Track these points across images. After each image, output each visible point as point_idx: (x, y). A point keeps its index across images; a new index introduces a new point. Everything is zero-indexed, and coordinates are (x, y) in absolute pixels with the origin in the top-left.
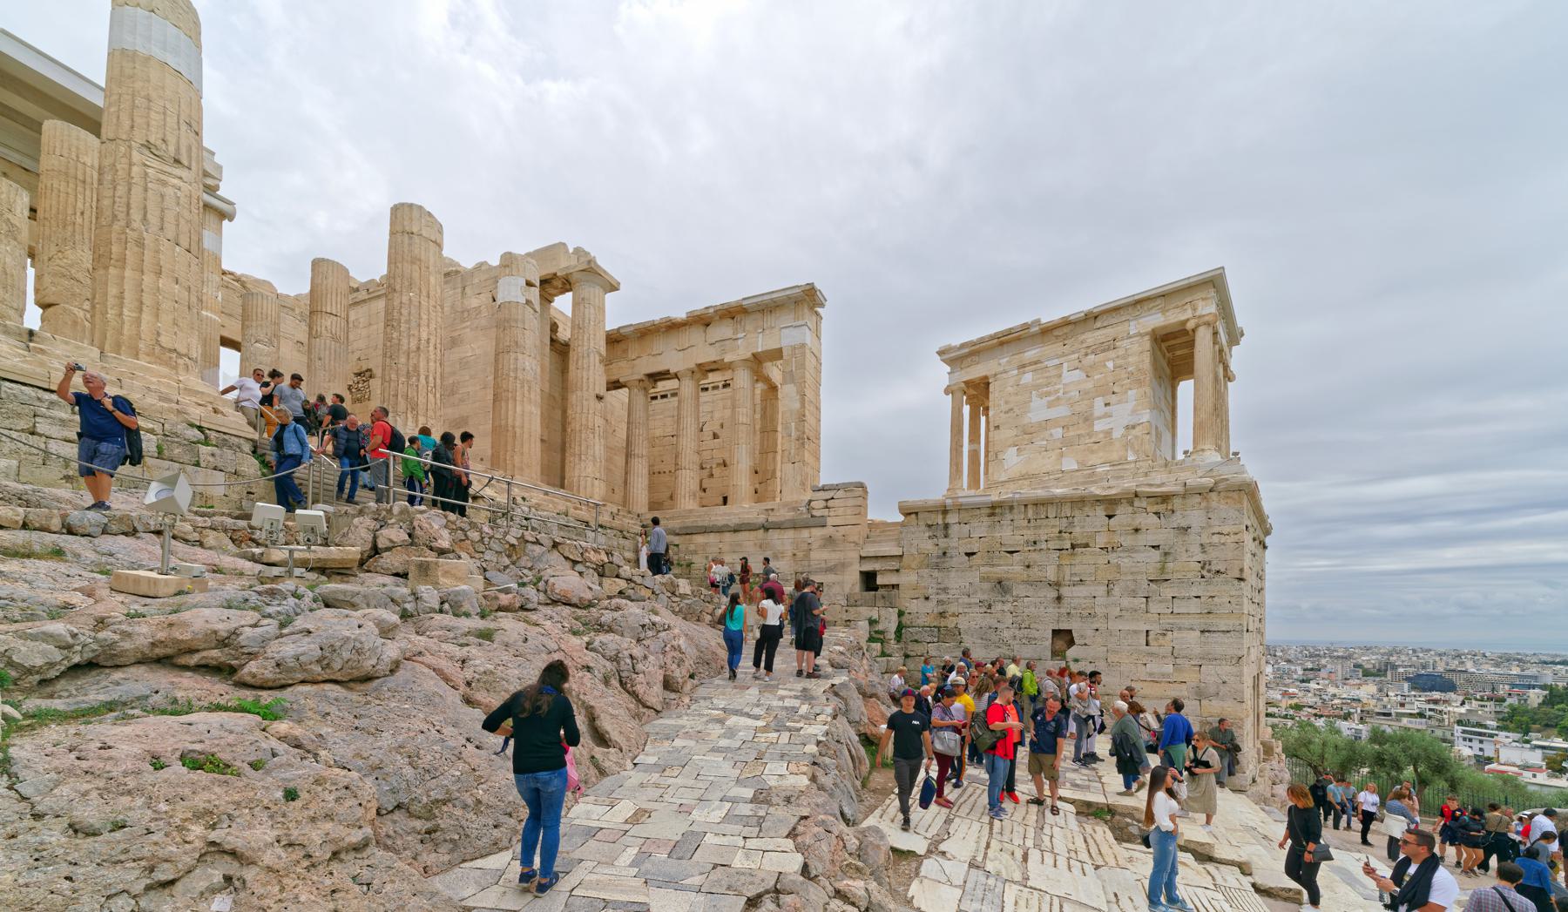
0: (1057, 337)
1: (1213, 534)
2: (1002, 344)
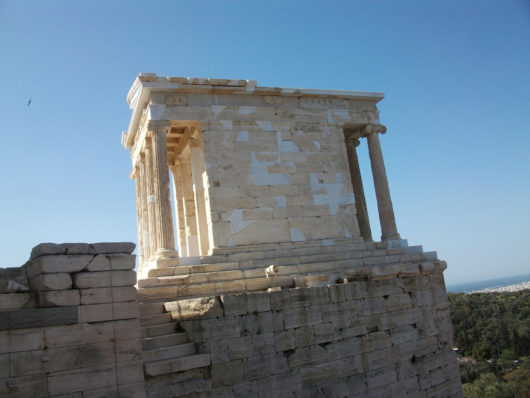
0: (268, 105)
1: (438, 310)
2: (213, 92)
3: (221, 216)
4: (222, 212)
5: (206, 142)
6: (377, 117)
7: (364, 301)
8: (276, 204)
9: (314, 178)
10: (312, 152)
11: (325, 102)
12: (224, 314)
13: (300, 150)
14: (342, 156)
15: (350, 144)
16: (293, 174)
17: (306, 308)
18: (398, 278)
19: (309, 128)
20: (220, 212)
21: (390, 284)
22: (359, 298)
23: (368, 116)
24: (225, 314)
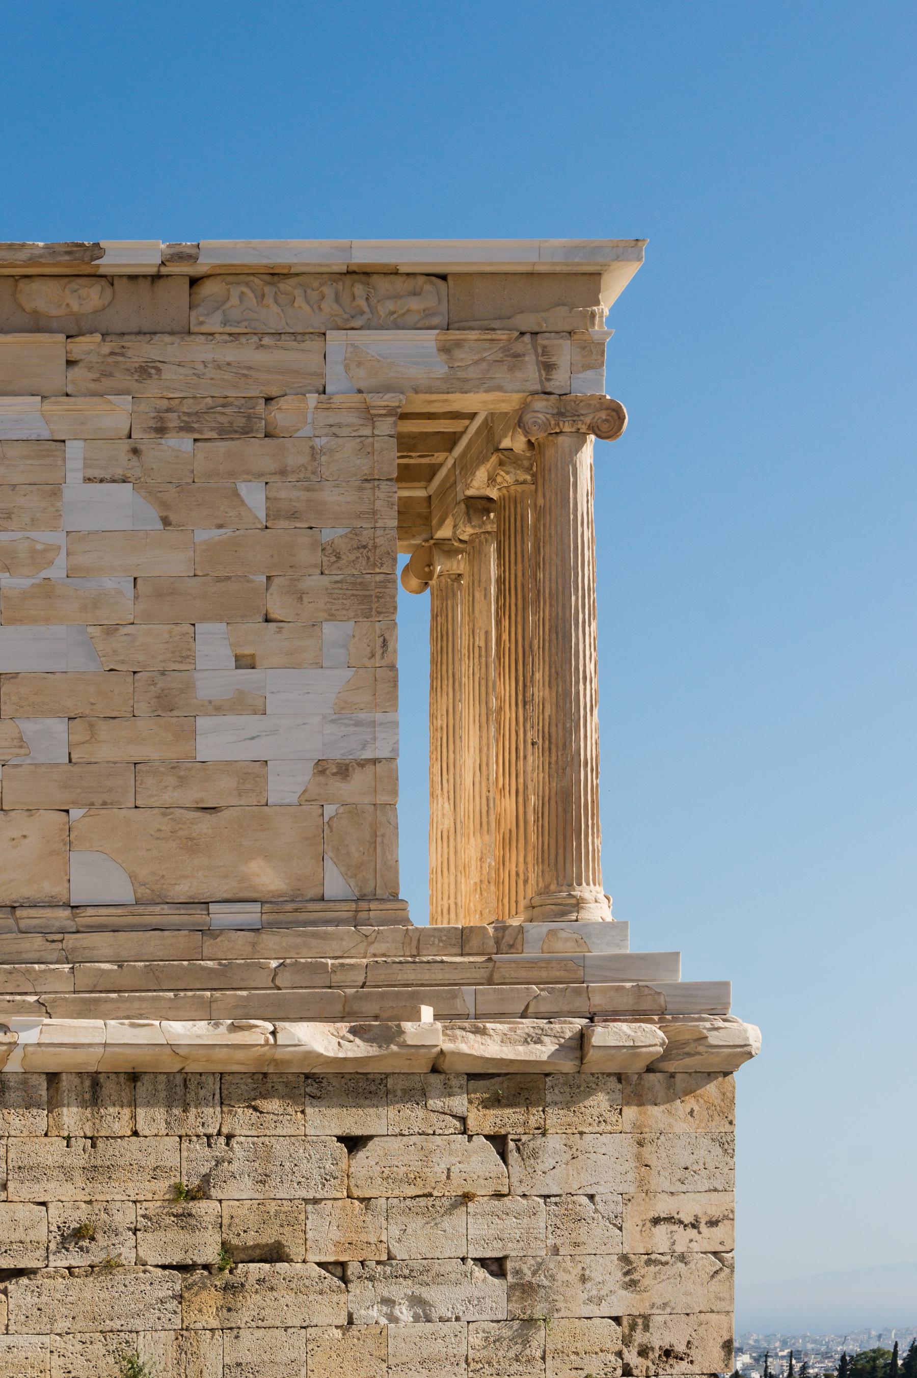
7: (227, 1144)
19: (223, 419)
21: (387, 1093)
22: (201, 1131)
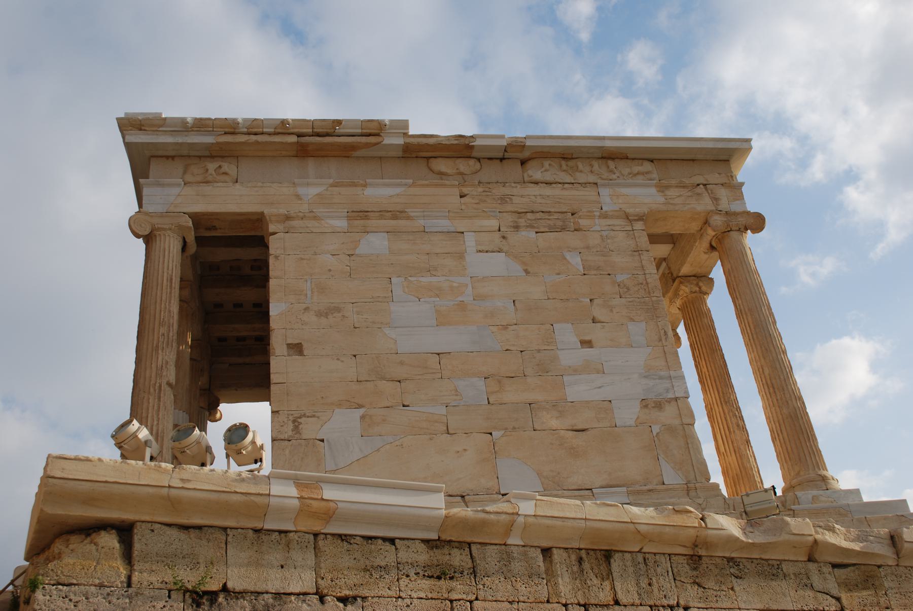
3: (301, 426)
4: (304, 415)
5: (277, 257)
6: (741, 197)
8: (458, 398)
9: (566, 334)
10: (558, 276)
11: (592, 167)
12: (129, 578)
13: (527, 272)
14: (644, 282)
15: (686, 287)
16: (505, 327)
17: (455, 603)
18: (816, 565)
19: (551, 223)
20: (295, 416)
22: (665, 602)
23: (712, 193)
24: (135, 578)
